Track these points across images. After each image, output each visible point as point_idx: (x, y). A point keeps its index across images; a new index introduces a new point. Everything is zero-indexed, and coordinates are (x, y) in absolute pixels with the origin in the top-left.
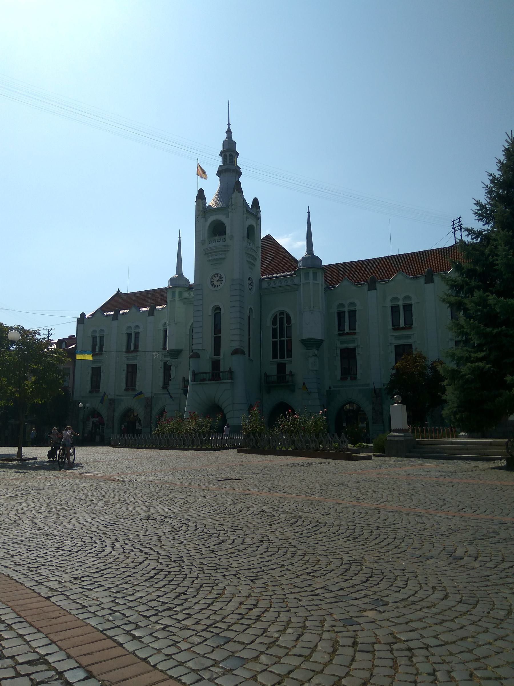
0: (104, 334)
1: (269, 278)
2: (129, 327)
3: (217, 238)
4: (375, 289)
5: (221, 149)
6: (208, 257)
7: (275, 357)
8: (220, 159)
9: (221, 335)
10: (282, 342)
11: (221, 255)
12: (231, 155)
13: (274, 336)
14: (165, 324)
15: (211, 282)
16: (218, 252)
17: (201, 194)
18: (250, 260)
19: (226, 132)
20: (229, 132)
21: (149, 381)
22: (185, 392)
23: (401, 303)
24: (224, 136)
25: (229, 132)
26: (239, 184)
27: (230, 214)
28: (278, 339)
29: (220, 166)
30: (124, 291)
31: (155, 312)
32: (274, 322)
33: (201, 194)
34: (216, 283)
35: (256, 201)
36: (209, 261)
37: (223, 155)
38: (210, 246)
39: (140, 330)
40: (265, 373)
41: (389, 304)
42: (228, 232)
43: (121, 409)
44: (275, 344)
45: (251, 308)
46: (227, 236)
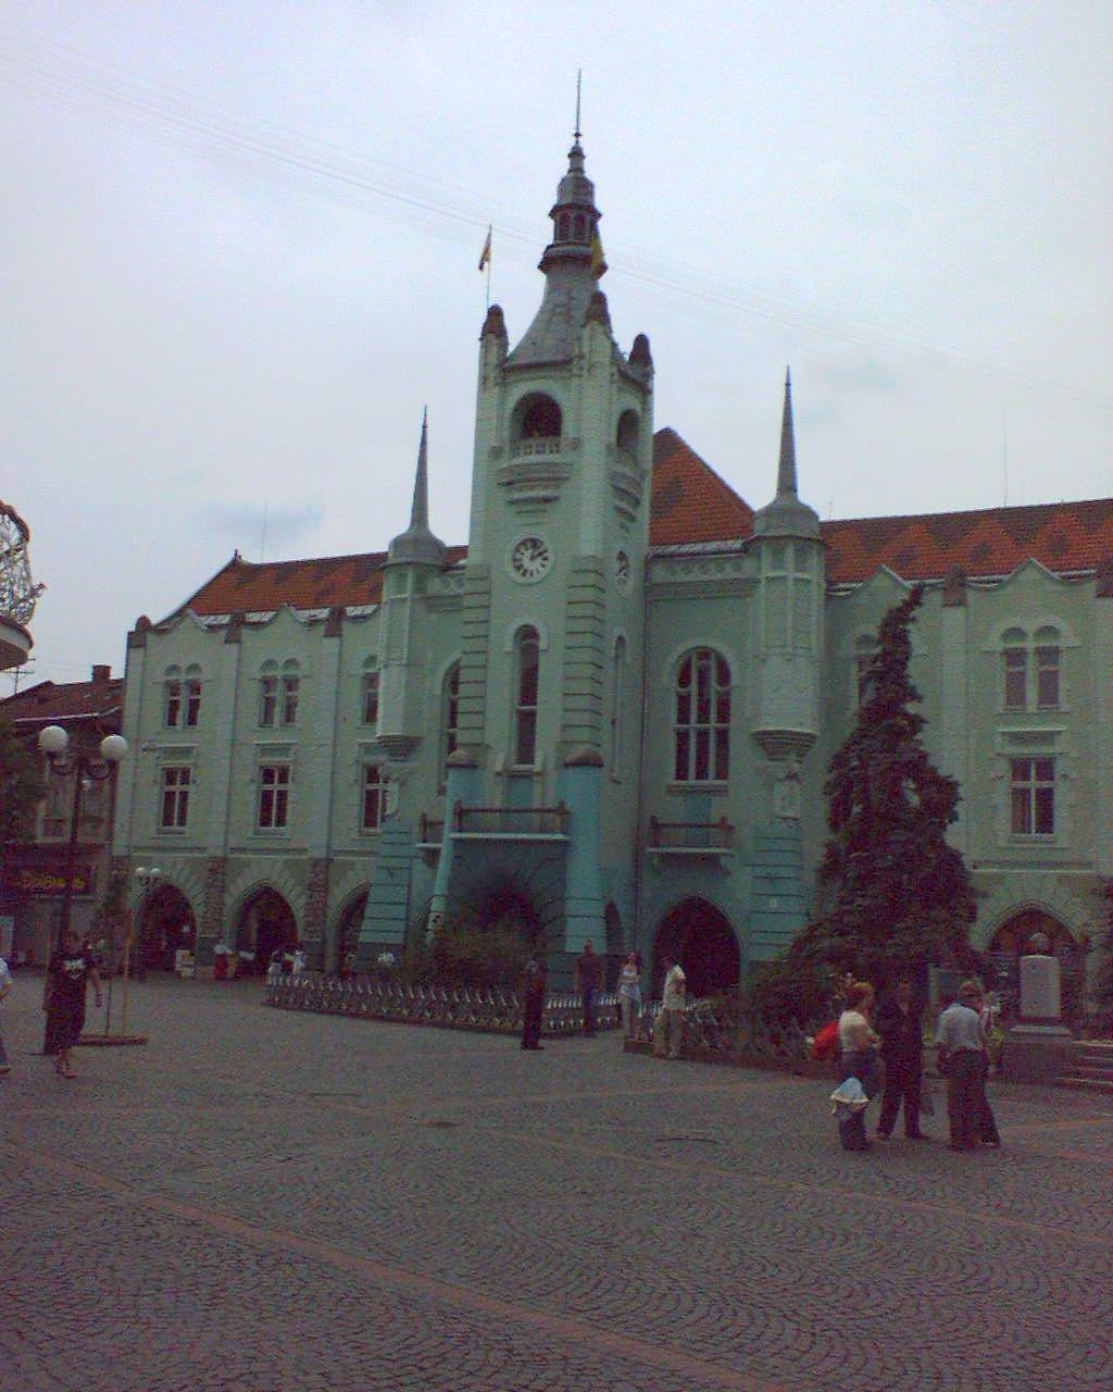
0: (202, 677)
1: (672, 555)
2: (270, 663)
3: (533, 442)
4: (961, 603)
5: (551, 199)
6: (510, 491)
7: (681, 773)
8: (551, 223)
9: (539, 708)
10: (703, 736)
13: (683, 716)
14: (371, 660)
15: (515, 560)
17: (494, 323)
18: (623, 505)
19: (569, 156)
20: (576, 154)
21: (320, 816)
22: (432, 857)
23: (1030, 644)
24: (563, 166)
25: (576, 154)
26: (600, 299)
28: (694, 724)
29: (548, 247)
30: (253, 557)
31: (346, 626)
32: (684, 679)
33: (494, 323)
34: (526, 562)
35: (641, 343)
36: (512, 502)
38: (516, 461)
39: (300, 673)
40: (653, 820)
41: (999, 646)
42: (569, 426)
43: (239, 888)
44: (682, 737)
45: (621, 639)
46: (563, 436)
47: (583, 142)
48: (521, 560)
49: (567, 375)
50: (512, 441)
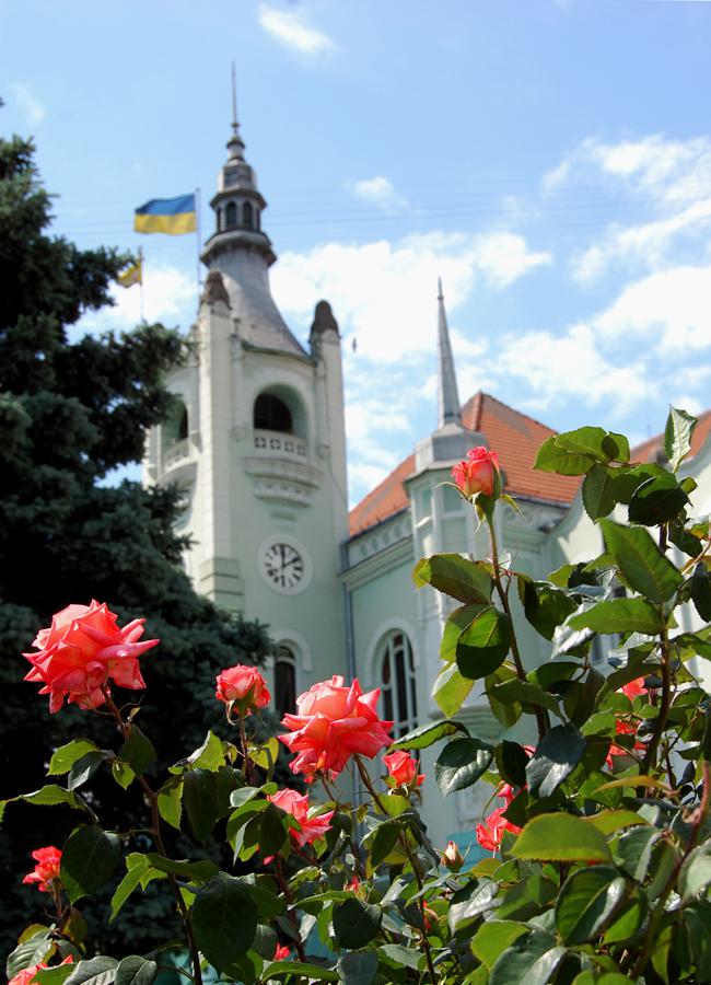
19: (229, 145)
20: (236, 143)
36: (261, 498)
37: (240, 202)
47: (244, 135)
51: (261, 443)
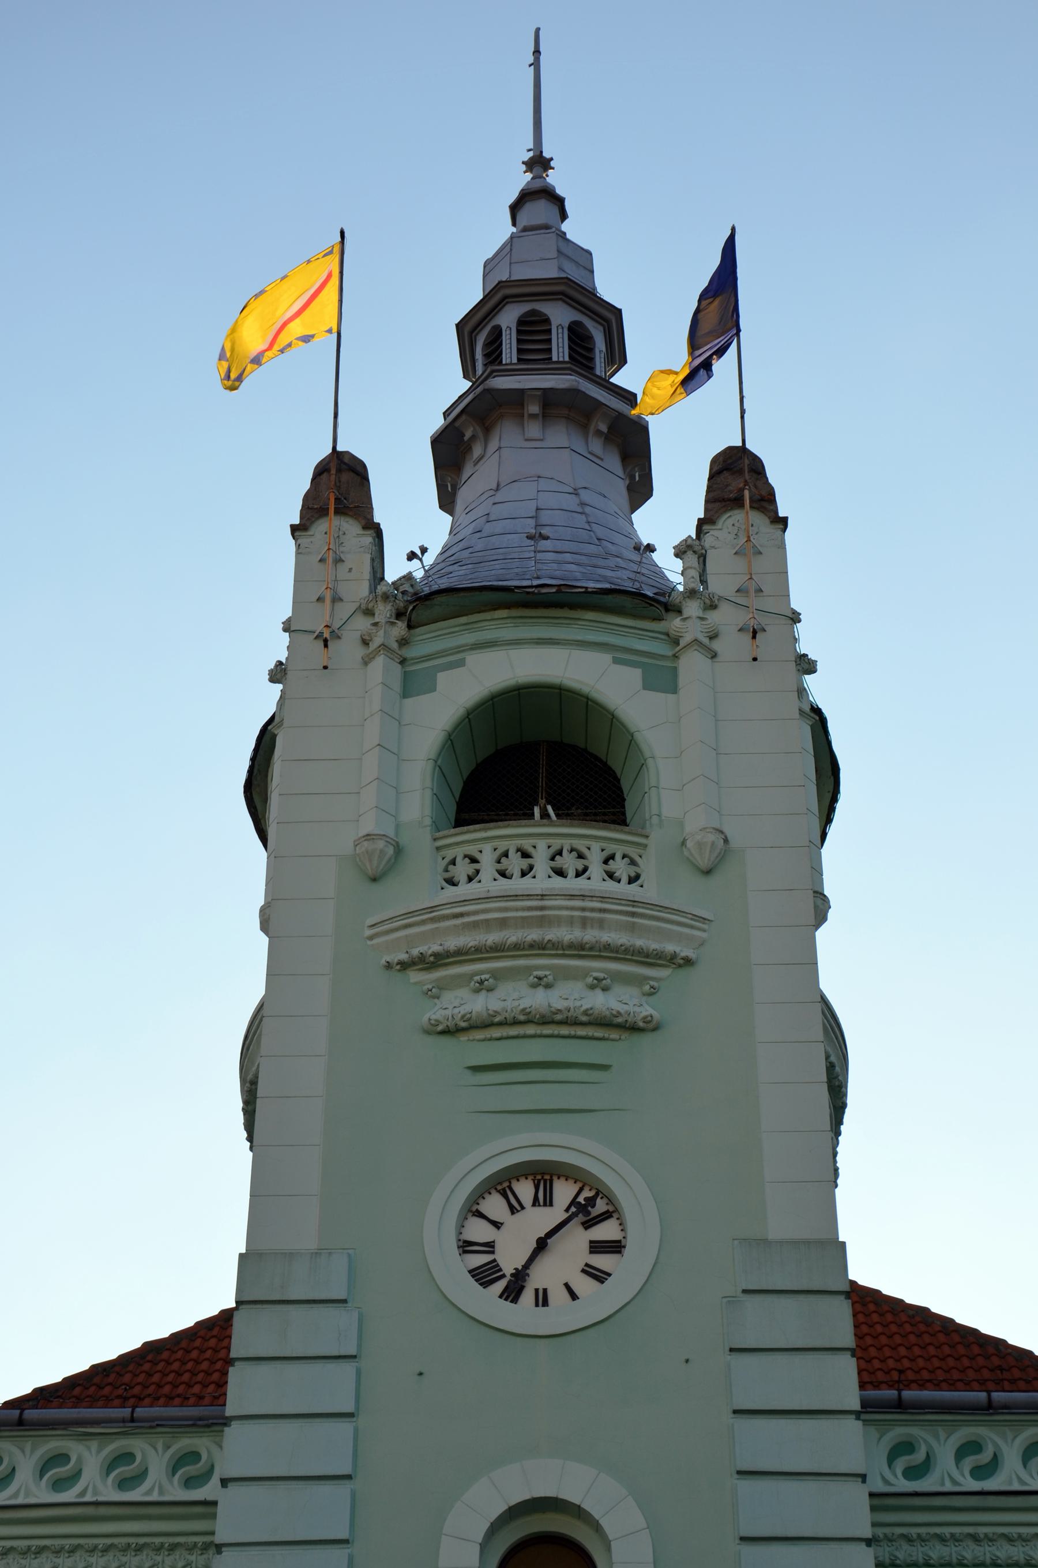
3: (542, 834)
11: (599, 985)
12: (578, 337)
15: (466, 1247)
16: (579, 950)
19: (515, 209)
20: (539, 201)
27: (692, 666)
37: (508, 319)
48: (489, 1247)
49: (661, 648)
50: (436, 827)
51: (463, 869)
